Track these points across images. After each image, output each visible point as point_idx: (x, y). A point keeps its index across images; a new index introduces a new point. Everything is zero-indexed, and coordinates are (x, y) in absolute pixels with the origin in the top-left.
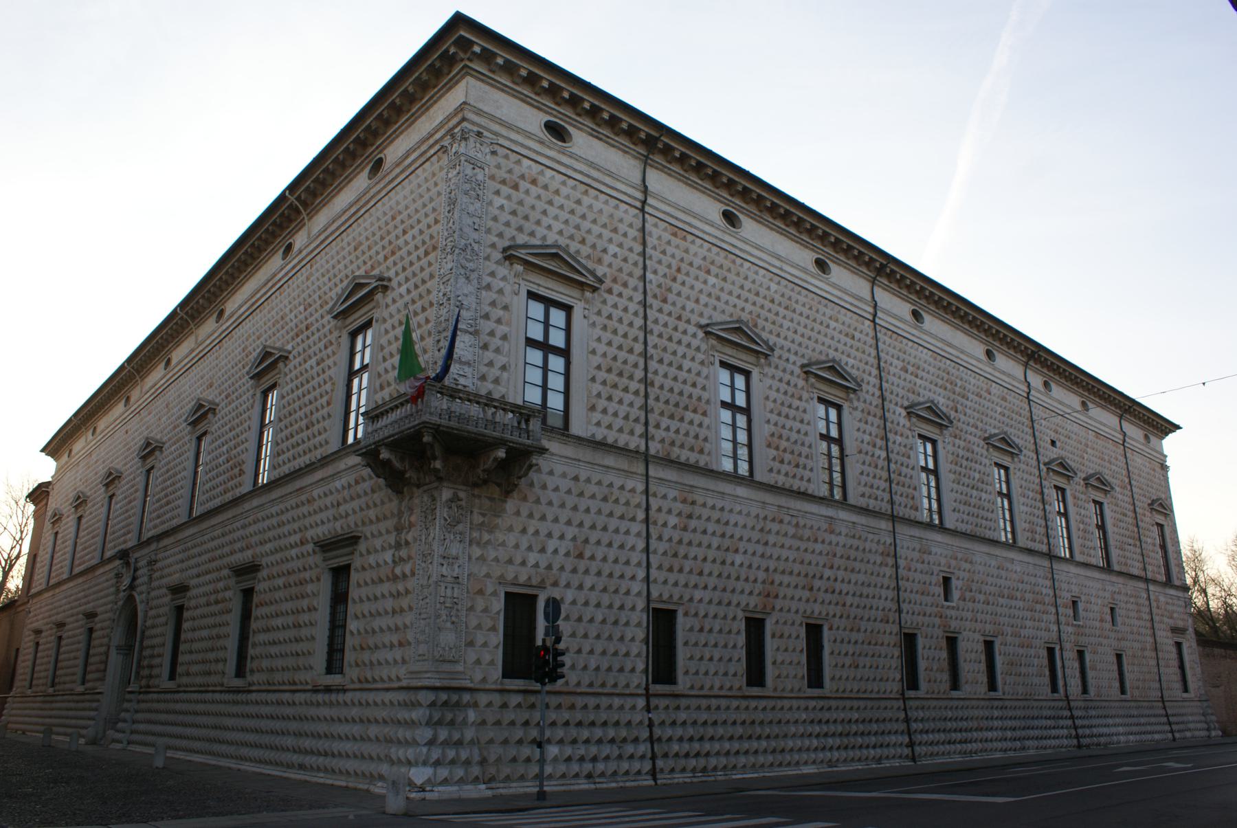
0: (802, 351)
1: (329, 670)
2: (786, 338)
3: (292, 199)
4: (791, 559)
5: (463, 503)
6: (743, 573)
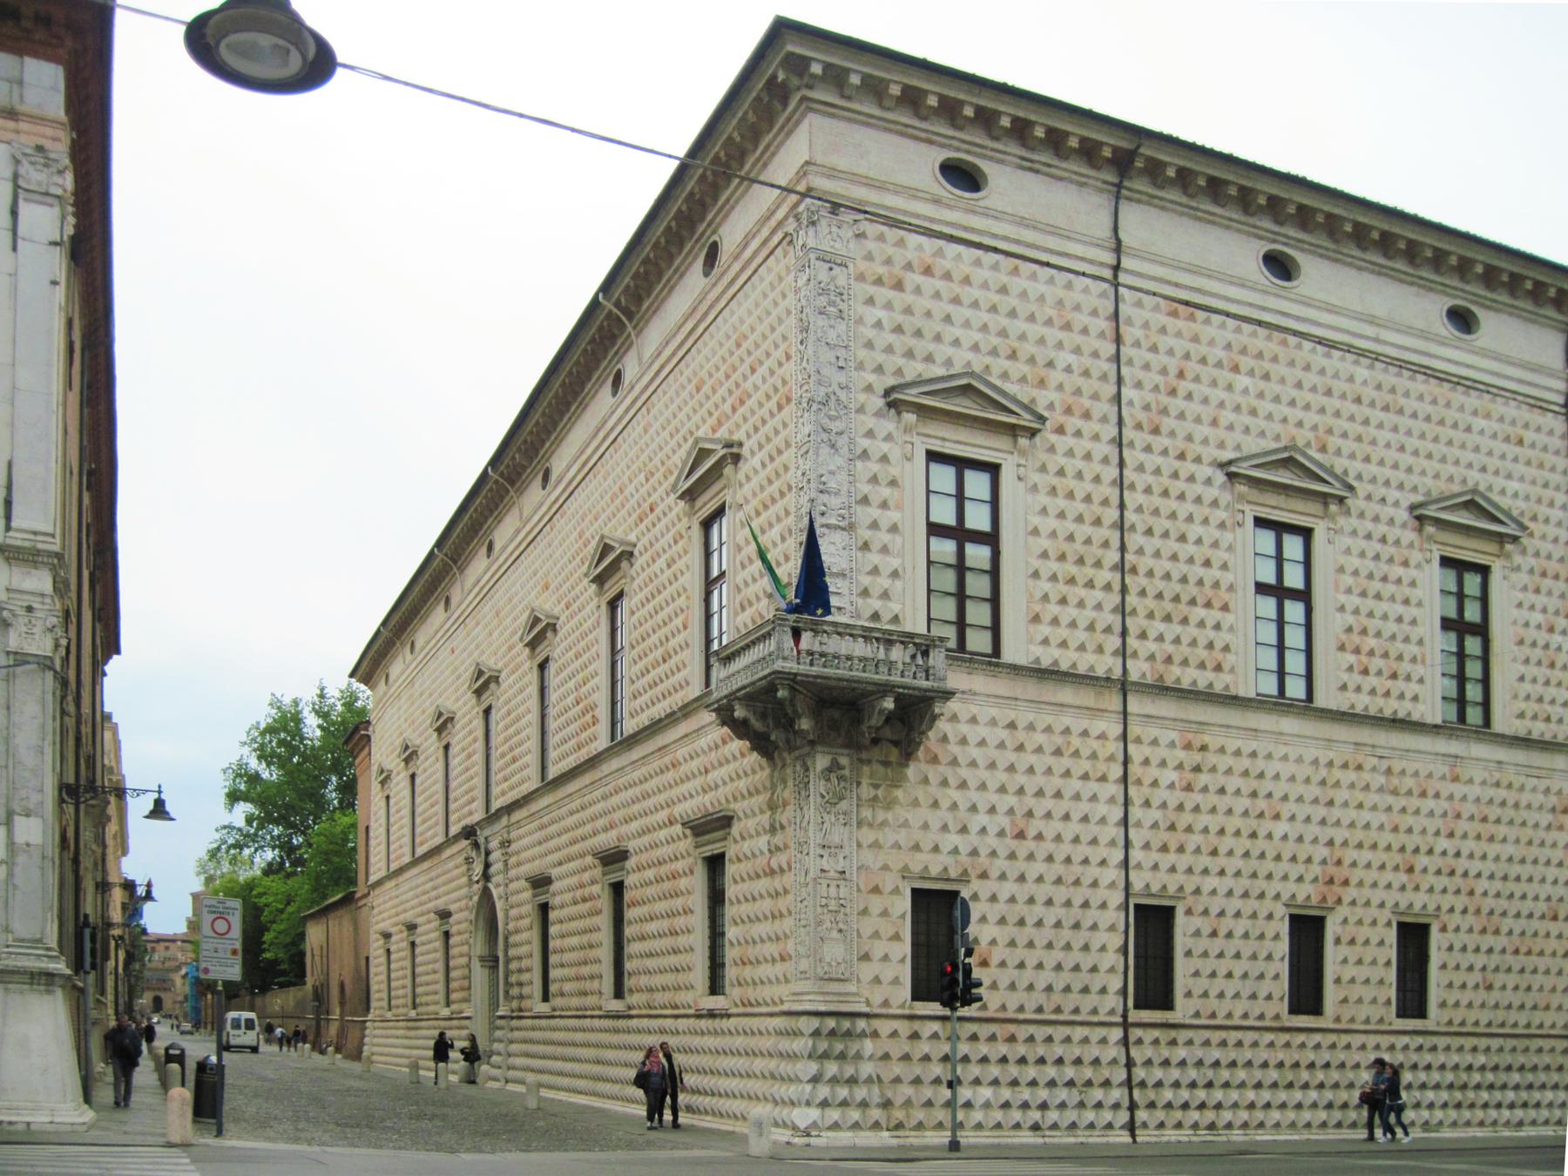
0: (1415, 479)
2: (1381, 463)
4: (1375, 825)
5: (846, 772)
6: (1288, 850)
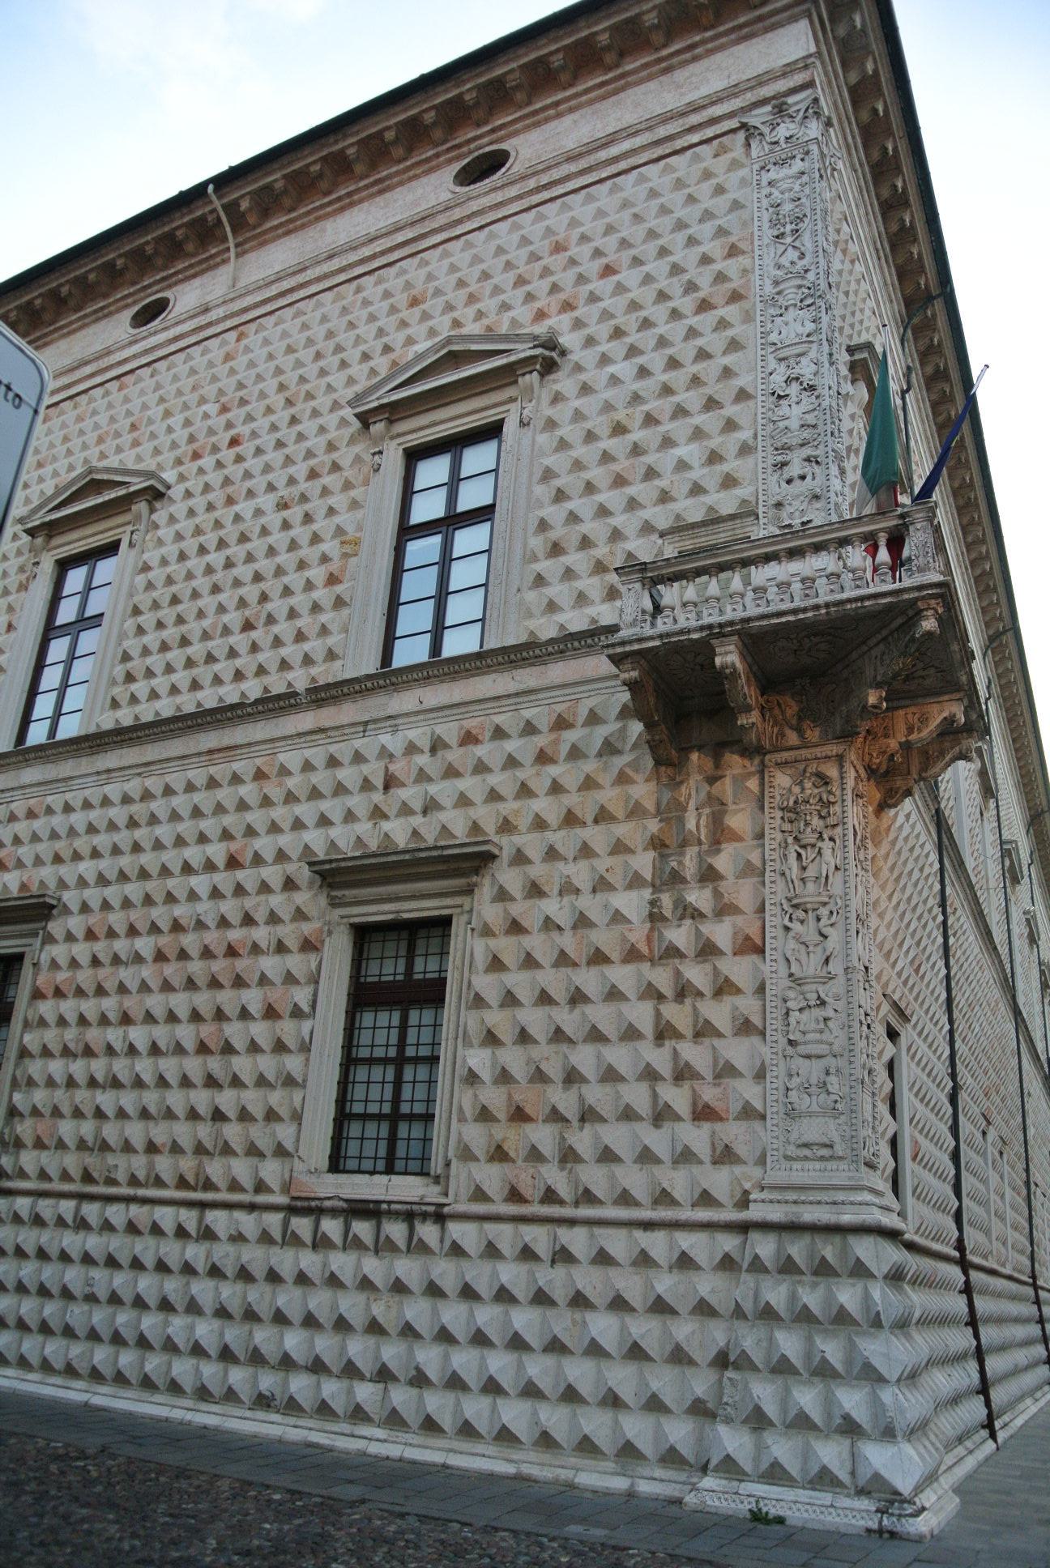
1: (336, 1164)
3: (217, 204)
